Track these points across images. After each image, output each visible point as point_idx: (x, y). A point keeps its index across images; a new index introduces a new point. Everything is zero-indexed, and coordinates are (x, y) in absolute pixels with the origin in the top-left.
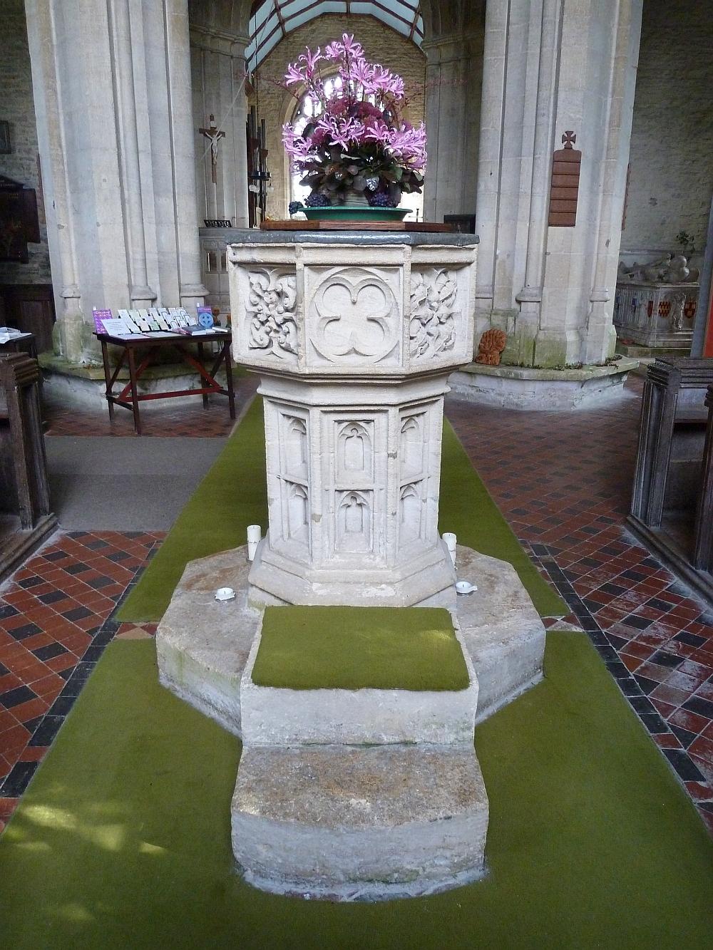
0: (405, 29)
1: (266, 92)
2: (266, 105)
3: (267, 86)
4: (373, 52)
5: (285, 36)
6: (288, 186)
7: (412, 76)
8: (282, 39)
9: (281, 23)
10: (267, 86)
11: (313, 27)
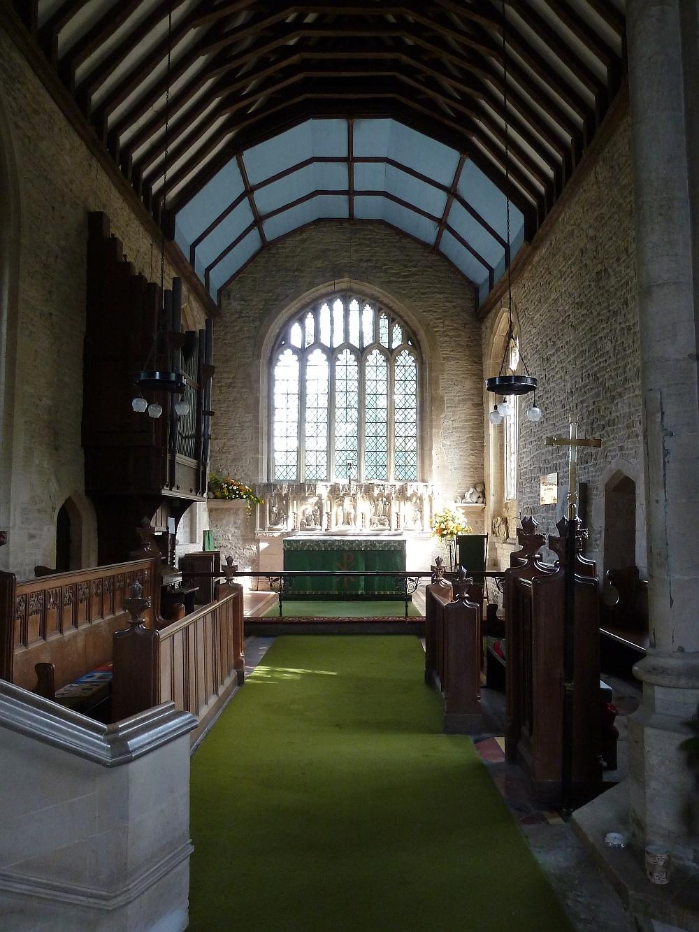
0: (427, 231)
1: (237, 316)
2: (238, 331)
3: (239, 307)
4: (386, 265)
5: (266, 246)
6: (265, 437)
7: (440, 293)
9: (258, 221)
10: (239, 307)
11: (304, 236)
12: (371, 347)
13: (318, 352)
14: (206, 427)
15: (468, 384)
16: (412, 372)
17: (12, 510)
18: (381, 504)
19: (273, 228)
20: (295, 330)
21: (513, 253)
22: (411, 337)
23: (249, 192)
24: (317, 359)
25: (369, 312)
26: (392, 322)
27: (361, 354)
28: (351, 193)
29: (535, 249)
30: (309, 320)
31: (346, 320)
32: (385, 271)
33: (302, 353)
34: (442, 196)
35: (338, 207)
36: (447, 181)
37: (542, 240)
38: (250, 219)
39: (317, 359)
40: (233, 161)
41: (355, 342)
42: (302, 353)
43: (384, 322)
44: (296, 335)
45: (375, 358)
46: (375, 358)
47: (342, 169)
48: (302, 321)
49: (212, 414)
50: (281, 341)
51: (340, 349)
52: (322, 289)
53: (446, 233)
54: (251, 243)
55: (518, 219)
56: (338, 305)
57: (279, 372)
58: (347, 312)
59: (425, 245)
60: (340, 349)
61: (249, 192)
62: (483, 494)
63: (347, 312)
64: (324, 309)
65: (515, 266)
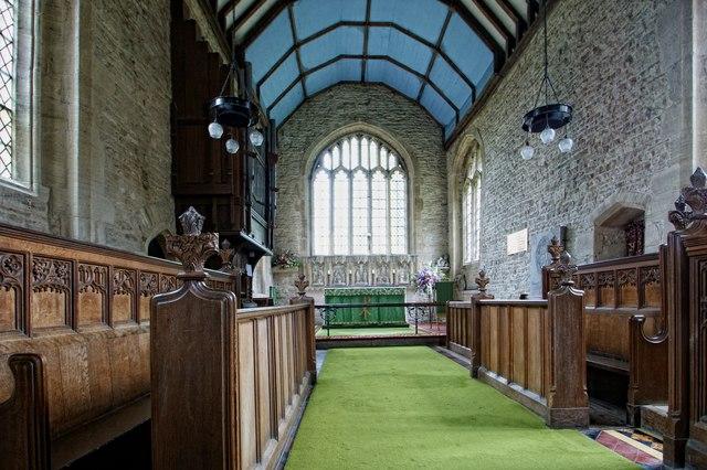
0: (412, 86)
5: (306, 99)
8: (303, 102)
9: (302, 77)
12: (376, 169)
13: (341, 172)
14: (273, 200)
15: (438, 191)
16: (402, 185)
17: (93, 226)
18: (384, 269)
19: (314, 82)
20: (326, 157)
21: (478, 95)
22: (401, 161)
23: (296, 46)
24: (341, 176)
25: (374, 146)
26: (389, 151)
27: (369, 173)
28: (365, 57)
29: (502, 77)
30: (336, 150)
31: (358, 152)
32: (385, 118)
33: (332, 173)
34: (428, 52)
35: (352, 69)
36: (433, 39)
37: (510, 67)
38: (296, 74)
39: (341, 176)
40: (285, 11)
41: (365, 165)
42: (332, 173)
43: (384, 152)
44: (328, 161)
45: (378, 176)
46: (378, 176)
47: (357, 32)
48: (330, 151)
49: (277, 190)
50: (317, 164)
51: (355, 170)
52: (344, 130)
53: (428, 87)
54: (295, 95)
55: (489, 57)
56: (354, 141)
57: (316, 185)
58: (360, 145)
59: (410, 100)
60: (355, 170)
61: (296, 46)
62: (448, 261)
63: (360, 145)
64: (345, 144)
65: (479, 103)
